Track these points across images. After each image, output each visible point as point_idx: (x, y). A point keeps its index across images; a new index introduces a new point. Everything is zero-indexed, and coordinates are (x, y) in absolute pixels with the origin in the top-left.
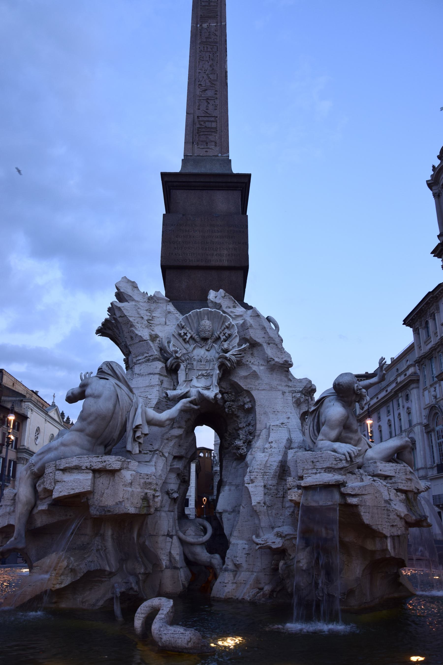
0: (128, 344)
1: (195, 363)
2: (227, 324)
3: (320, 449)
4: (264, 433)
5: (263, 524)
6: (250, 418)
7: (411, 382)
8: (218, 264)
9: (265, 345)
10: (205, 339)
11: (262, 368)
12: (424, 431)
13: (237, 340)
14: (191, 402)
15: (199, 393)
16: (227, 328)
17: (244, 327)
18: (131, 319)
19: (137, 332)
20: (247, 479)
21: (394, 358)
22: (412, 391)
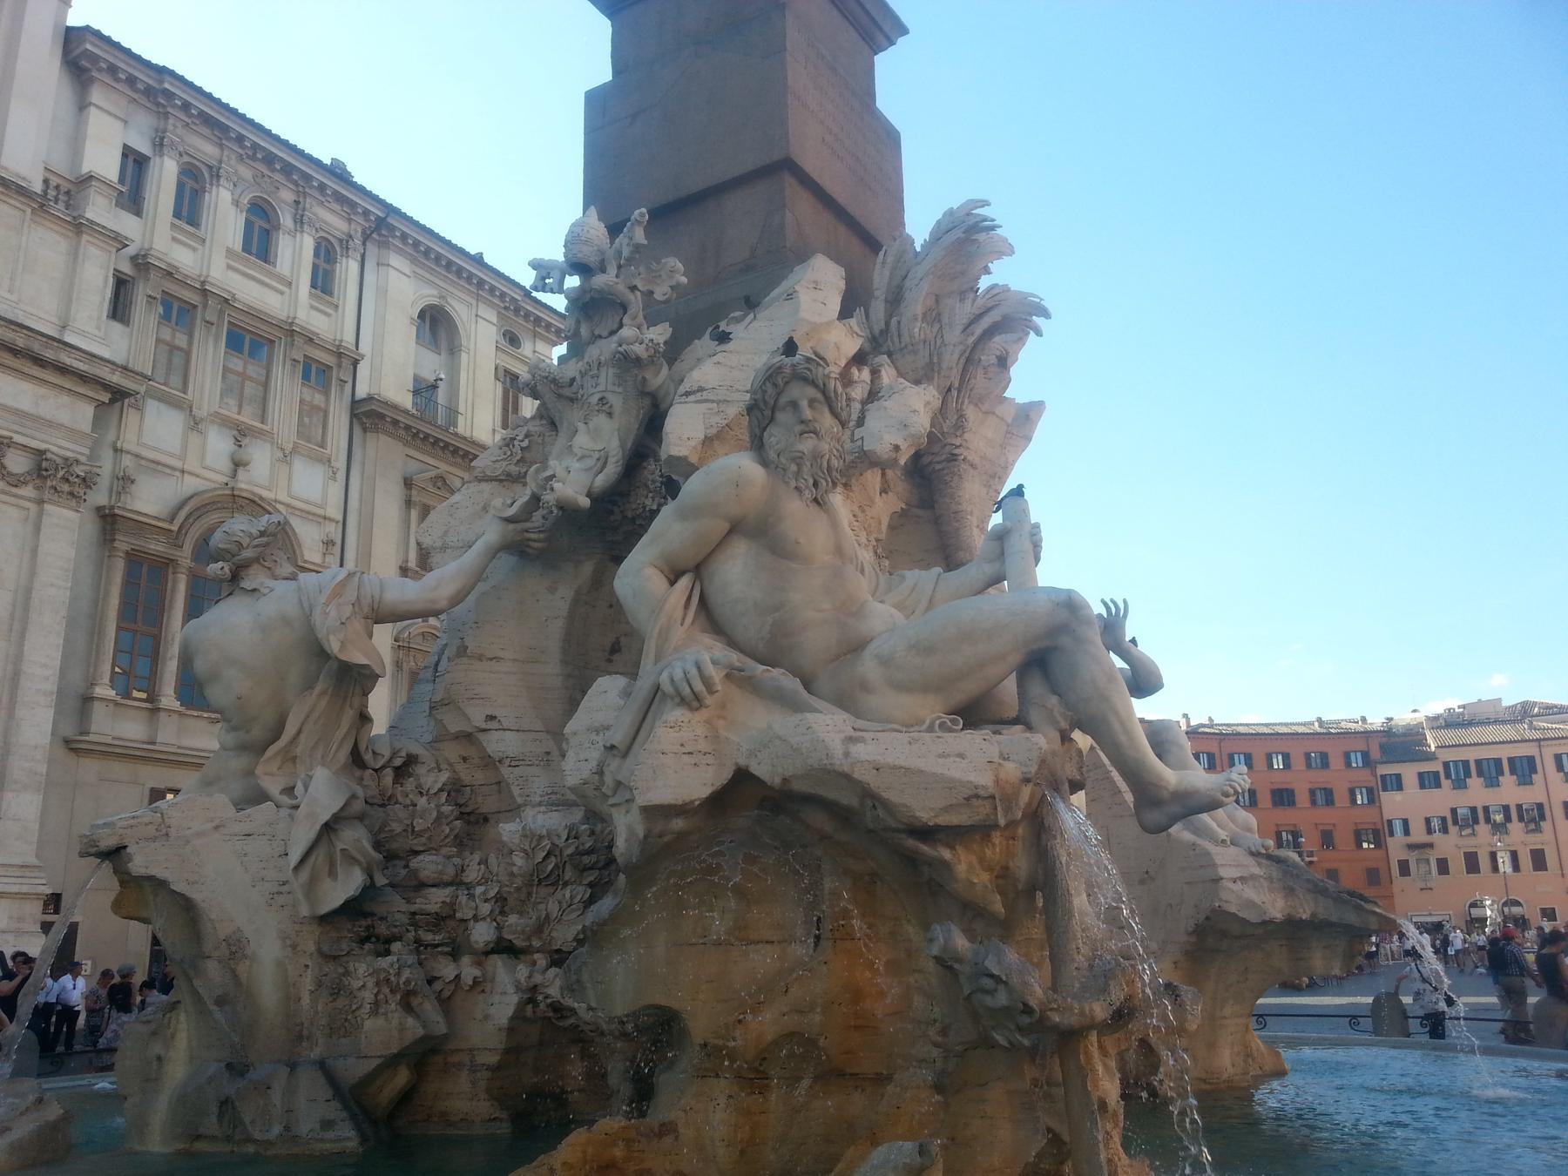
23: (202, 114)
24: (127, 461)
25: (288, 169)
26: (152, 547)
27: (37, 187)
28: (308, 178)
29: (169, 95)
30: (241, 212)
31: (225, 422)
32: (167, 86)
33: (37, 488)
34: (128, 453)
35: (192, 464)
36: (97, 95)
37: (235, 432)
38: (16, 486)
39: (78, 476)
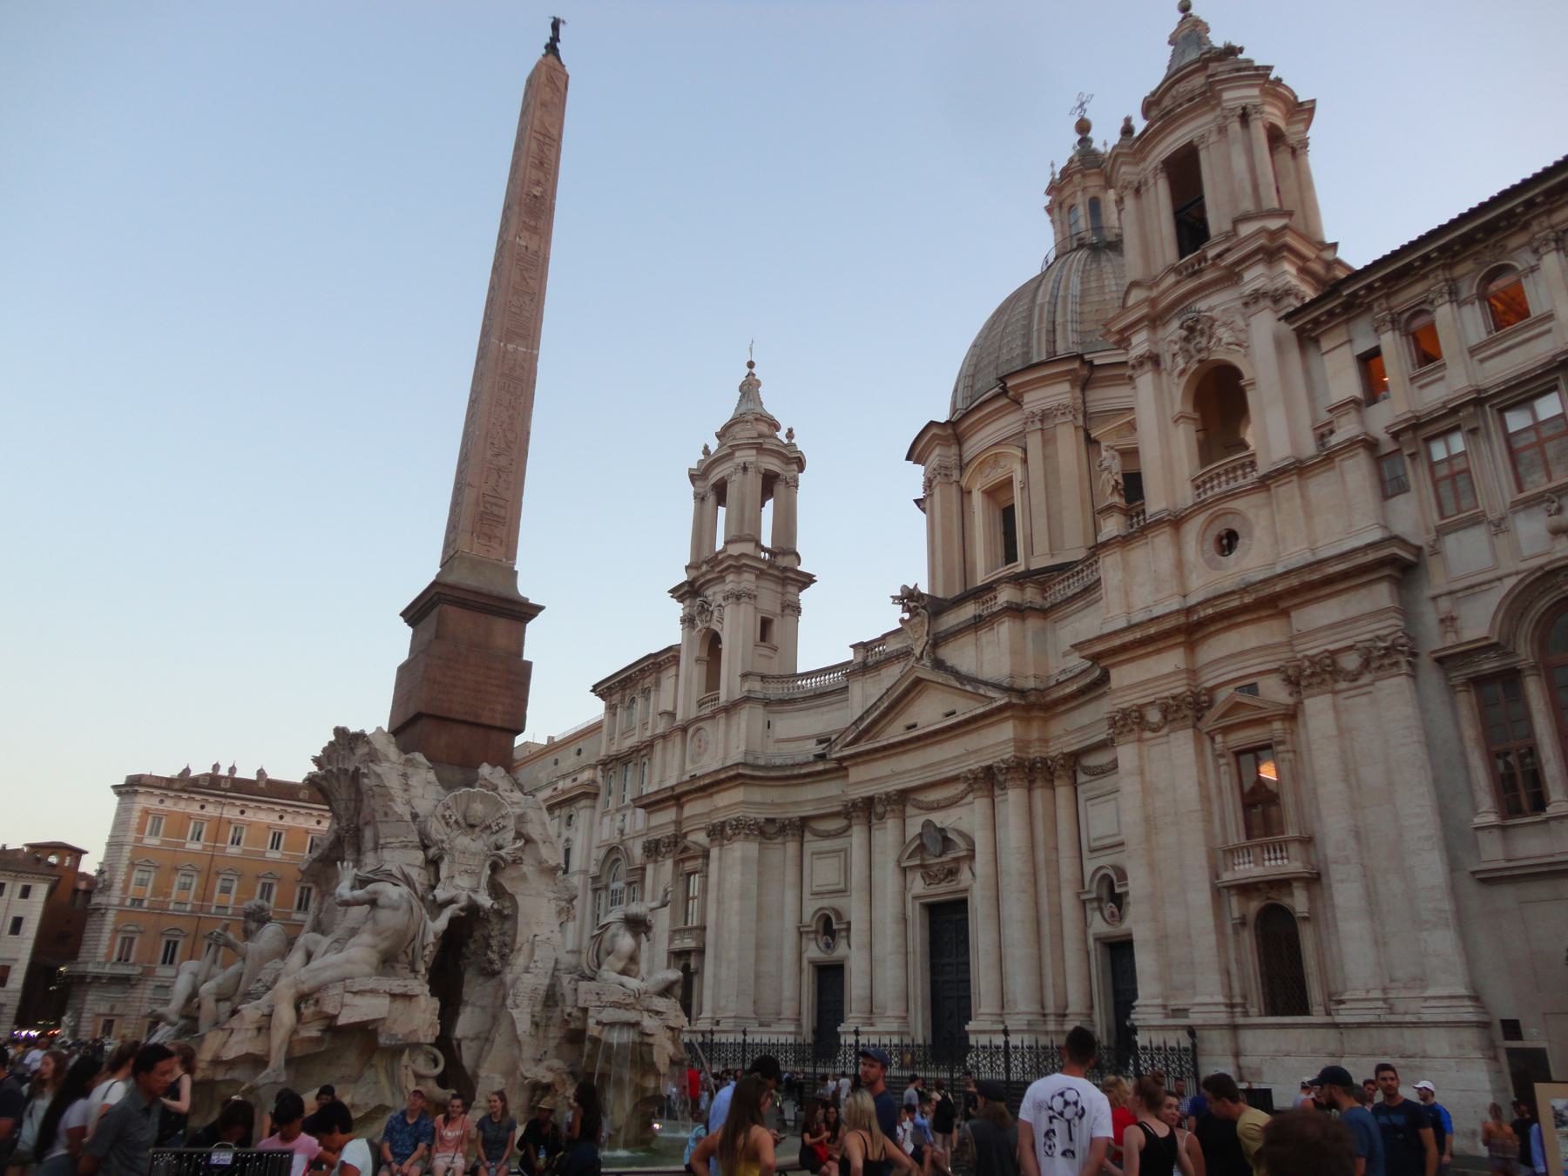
0: (378, 819)
1: (457, 854)
2: (503, 813)
3: (605, 980)
4: (526, 948)
5: (524, 1056)
6: (507, 925)
7: (585, 795)
8: (488, 722)
9: (541, 844)
10: (472, 826)
11: (531, 869)
12: (589, 886)
13: (512, 834)
14: (462, 909)
15: (469, 897)
16: (503, 817)
17: (521, 818)
18: (392, 791)
19: (397, 809)
20: (509, 1002)
21: (553, 738)
22: (581, 812)
23: (1385, 279)
24: (1445, 605)
25: (1490, 229)
26: (1486, 667)
27: (1309, 448)
28: (1511, 213)
29: (1354, 295)
30: (1473, 304)
31: (1528, 504)
32: (1345, 293)
33: (1370, 672)
34: (1440, 596)
35: (1508, 566)
36: (1326, 344)
37: (1545, 505)
38: (1353, 681)
39: (1386, 648)
